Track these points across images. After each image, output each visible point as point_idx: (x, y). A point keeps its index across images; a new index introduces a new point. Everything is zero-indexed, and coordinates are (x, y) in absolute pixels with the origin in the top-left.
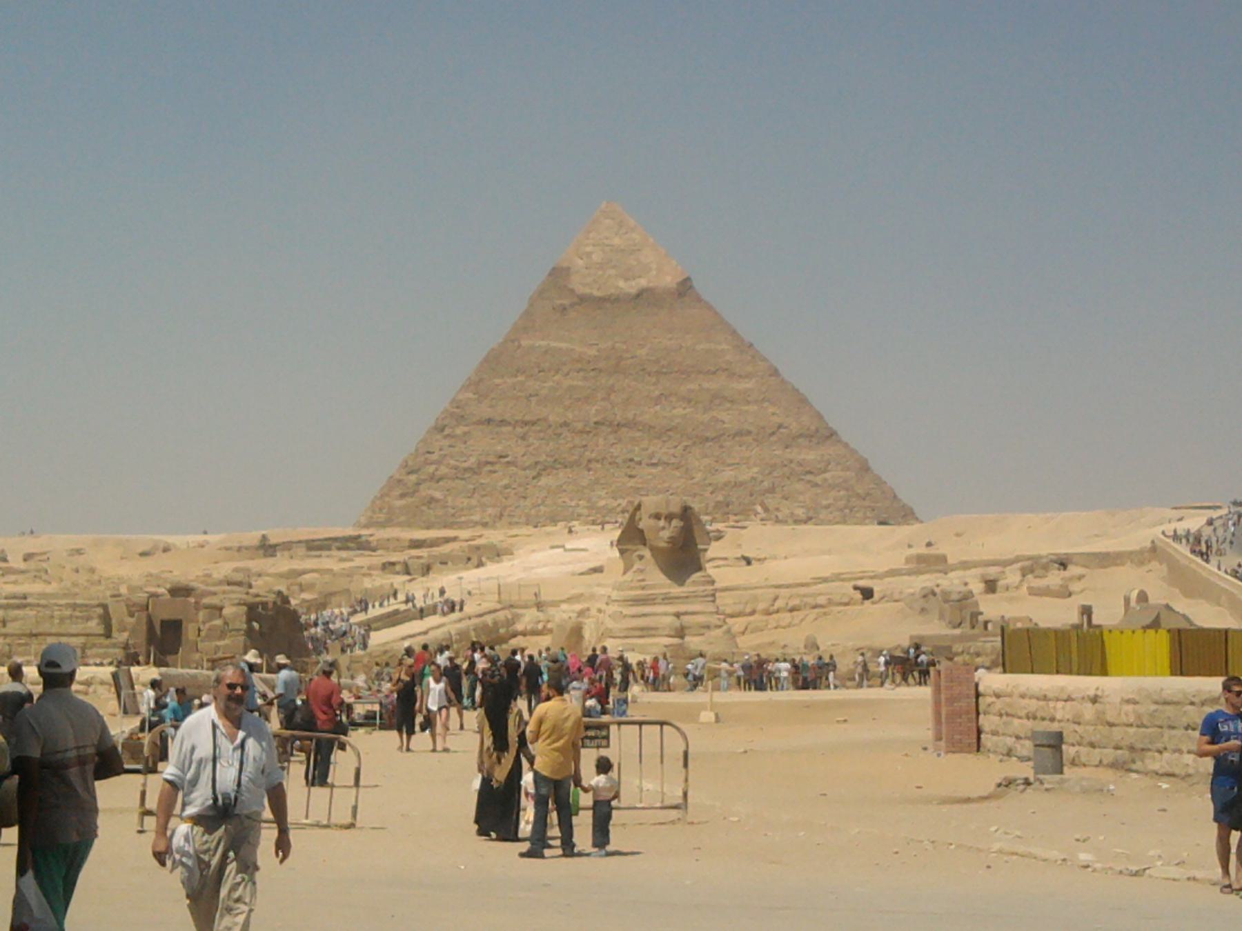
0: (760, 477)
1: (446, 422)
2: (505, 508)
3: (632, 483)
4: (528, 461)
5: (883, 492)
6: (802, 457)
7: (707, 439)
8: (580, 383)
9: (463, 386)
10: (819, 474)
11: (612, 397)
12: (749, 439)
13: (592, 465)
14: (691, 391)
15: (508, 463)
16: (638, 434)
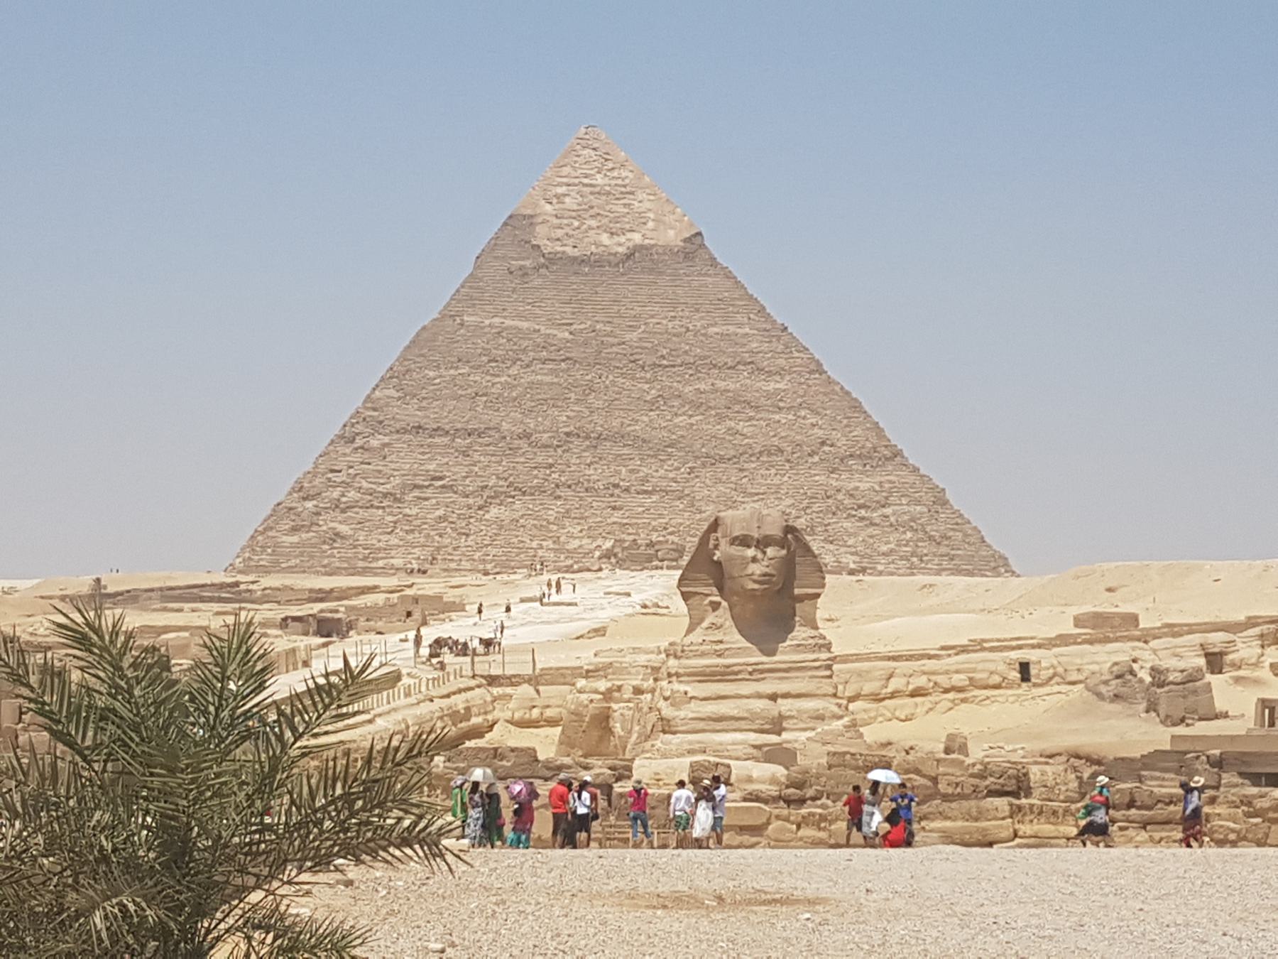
1: (359, 428)
2: (438, 549)
3: (616, 517)
5: (966, 535)
6: (852, 485)
7: (722, 458)
8: (548, 379)
9: (382, 379)
10: (874, 510)
11: (591, 399)
12: (779, 459)
15: (443, 487)
16: (625, 451)
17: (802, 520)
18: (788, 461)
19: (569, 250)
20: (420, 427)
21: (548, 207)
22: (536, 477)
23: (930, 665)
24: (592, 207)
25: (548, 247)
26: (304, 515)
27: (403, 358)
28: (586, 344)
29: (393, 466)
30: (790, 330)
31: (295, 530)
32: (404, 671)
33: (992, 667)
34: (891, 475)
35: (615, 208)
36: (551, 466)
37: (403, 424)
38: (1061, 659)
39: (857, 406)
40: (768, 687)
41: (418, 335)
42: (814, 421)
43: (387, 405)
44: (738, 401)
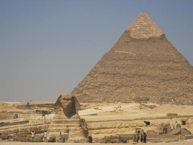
0: (180, 92)
1: (92, 73)
2: (106, 98)
3: (143, 92)
4: (114, 84)
8: (131, 63)
11: (139, 68)
12: (177, 81)
13: (132, 86)
14: (162, 66)
15: (108, 85)
16: (146, 78)
17: (181, 93)
18: (179, 81)
19: (137, 38)
20: (104, 73)
21: (134, 29)
22: (127, 83)
23: (130, 122)
24: (142, 29)
25: (133, 37)
26: (80, 90)
27: (102, 59)
29: (98, 80)
30: (182, 54)
31: (78, 93)
32: (29, 121)
33: (141, 123)
35: (148, 29)
36: (131, 81)
37: (101, 72)
38: (155, 122)
40: (67, 125)
41: (105, 54)
42: (185, 72)
43: (98, 68)
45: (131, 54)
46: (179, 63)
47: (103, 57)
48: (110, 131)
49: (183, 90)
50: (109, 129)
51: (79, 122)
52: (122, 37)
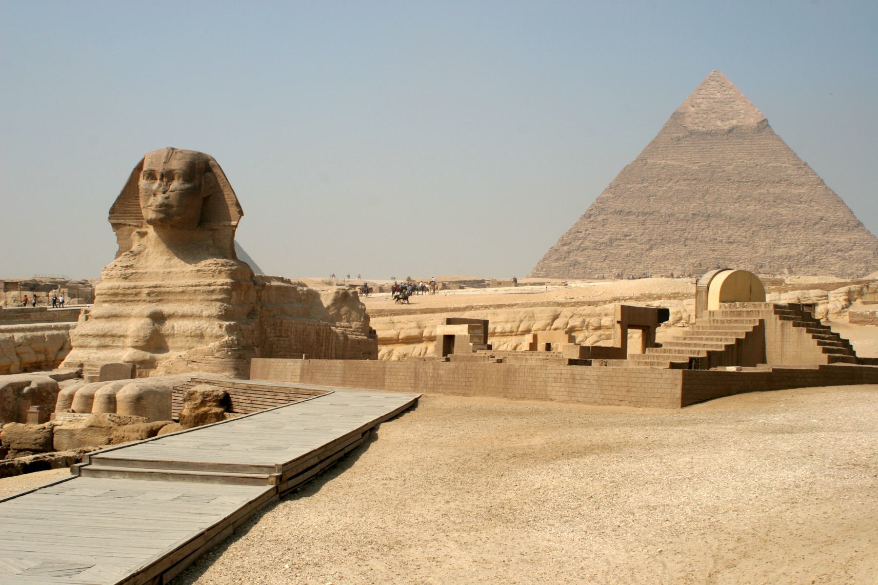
4: (646, 238)
6: (834, 240)
7: (769, 227)
11: (706, 198)
13: (688, 242)
14: (760, 194)
16: (722, 223)
19: (700, 128)
23: (587, 310)
25: (691, 127)
28: (705, 172)
31: (557, 260)
34: (855, 236)
39: (841, 202)
44: (778, 200)
45: (686, 166)
46: (802, 185)
47: (619, 176)
48: (505, 346)
49: (813, 250)
50: (504, 339)
51: (223, 296)
52: (665, 128)
